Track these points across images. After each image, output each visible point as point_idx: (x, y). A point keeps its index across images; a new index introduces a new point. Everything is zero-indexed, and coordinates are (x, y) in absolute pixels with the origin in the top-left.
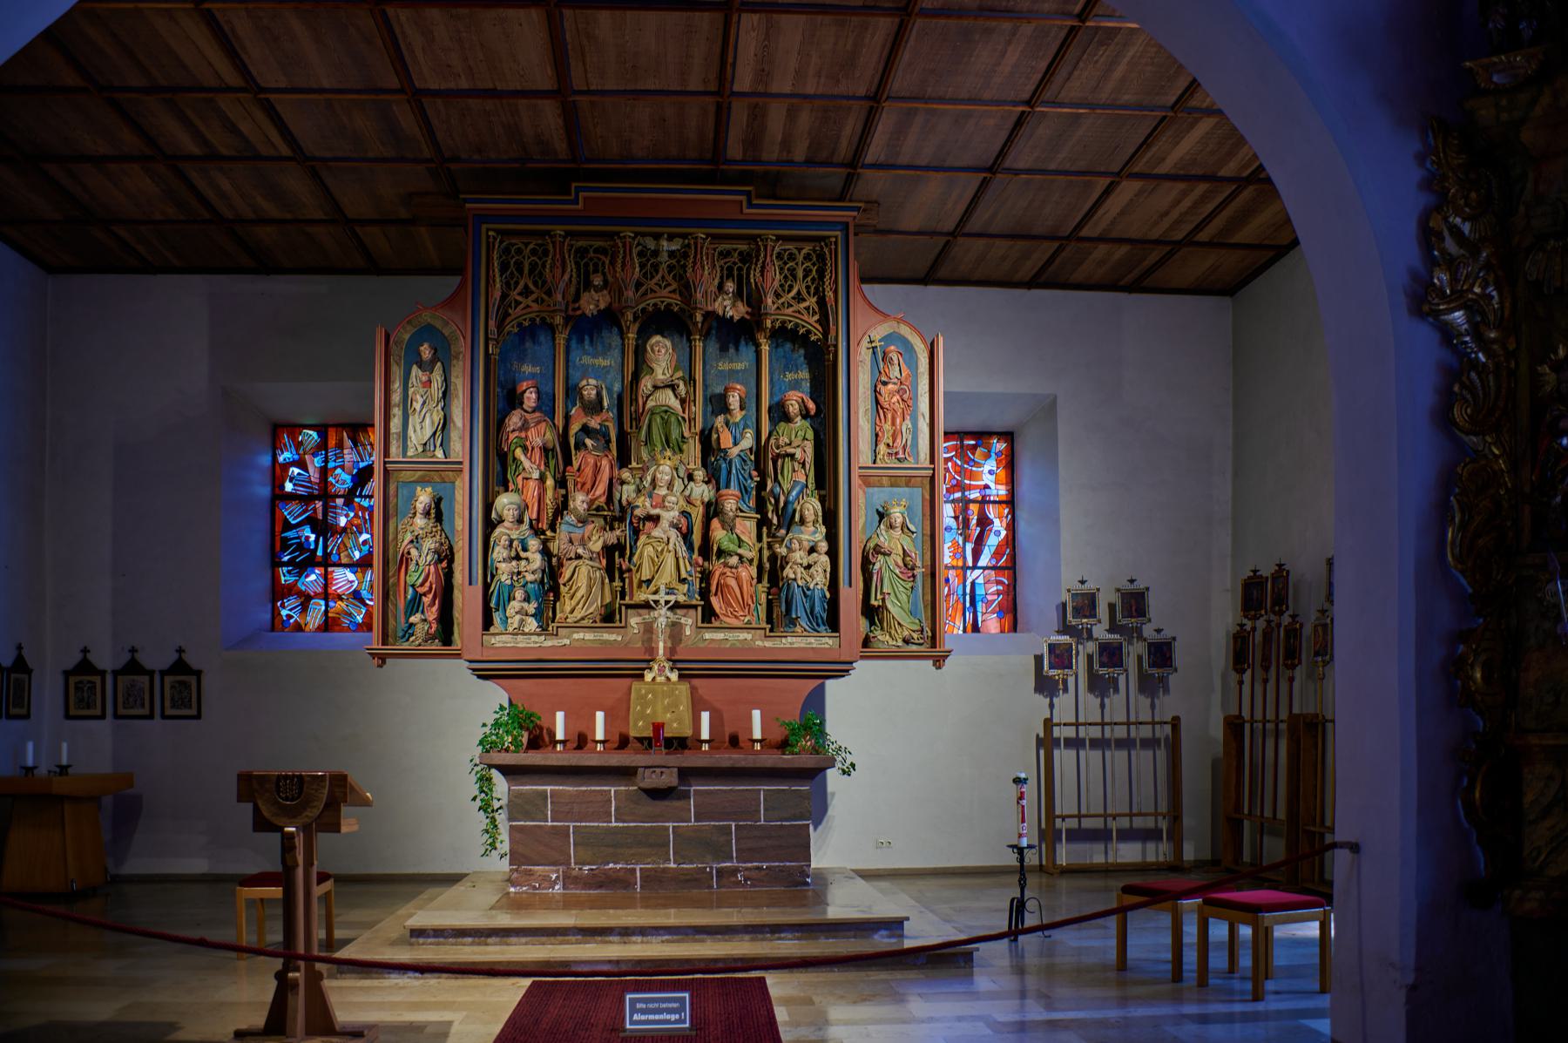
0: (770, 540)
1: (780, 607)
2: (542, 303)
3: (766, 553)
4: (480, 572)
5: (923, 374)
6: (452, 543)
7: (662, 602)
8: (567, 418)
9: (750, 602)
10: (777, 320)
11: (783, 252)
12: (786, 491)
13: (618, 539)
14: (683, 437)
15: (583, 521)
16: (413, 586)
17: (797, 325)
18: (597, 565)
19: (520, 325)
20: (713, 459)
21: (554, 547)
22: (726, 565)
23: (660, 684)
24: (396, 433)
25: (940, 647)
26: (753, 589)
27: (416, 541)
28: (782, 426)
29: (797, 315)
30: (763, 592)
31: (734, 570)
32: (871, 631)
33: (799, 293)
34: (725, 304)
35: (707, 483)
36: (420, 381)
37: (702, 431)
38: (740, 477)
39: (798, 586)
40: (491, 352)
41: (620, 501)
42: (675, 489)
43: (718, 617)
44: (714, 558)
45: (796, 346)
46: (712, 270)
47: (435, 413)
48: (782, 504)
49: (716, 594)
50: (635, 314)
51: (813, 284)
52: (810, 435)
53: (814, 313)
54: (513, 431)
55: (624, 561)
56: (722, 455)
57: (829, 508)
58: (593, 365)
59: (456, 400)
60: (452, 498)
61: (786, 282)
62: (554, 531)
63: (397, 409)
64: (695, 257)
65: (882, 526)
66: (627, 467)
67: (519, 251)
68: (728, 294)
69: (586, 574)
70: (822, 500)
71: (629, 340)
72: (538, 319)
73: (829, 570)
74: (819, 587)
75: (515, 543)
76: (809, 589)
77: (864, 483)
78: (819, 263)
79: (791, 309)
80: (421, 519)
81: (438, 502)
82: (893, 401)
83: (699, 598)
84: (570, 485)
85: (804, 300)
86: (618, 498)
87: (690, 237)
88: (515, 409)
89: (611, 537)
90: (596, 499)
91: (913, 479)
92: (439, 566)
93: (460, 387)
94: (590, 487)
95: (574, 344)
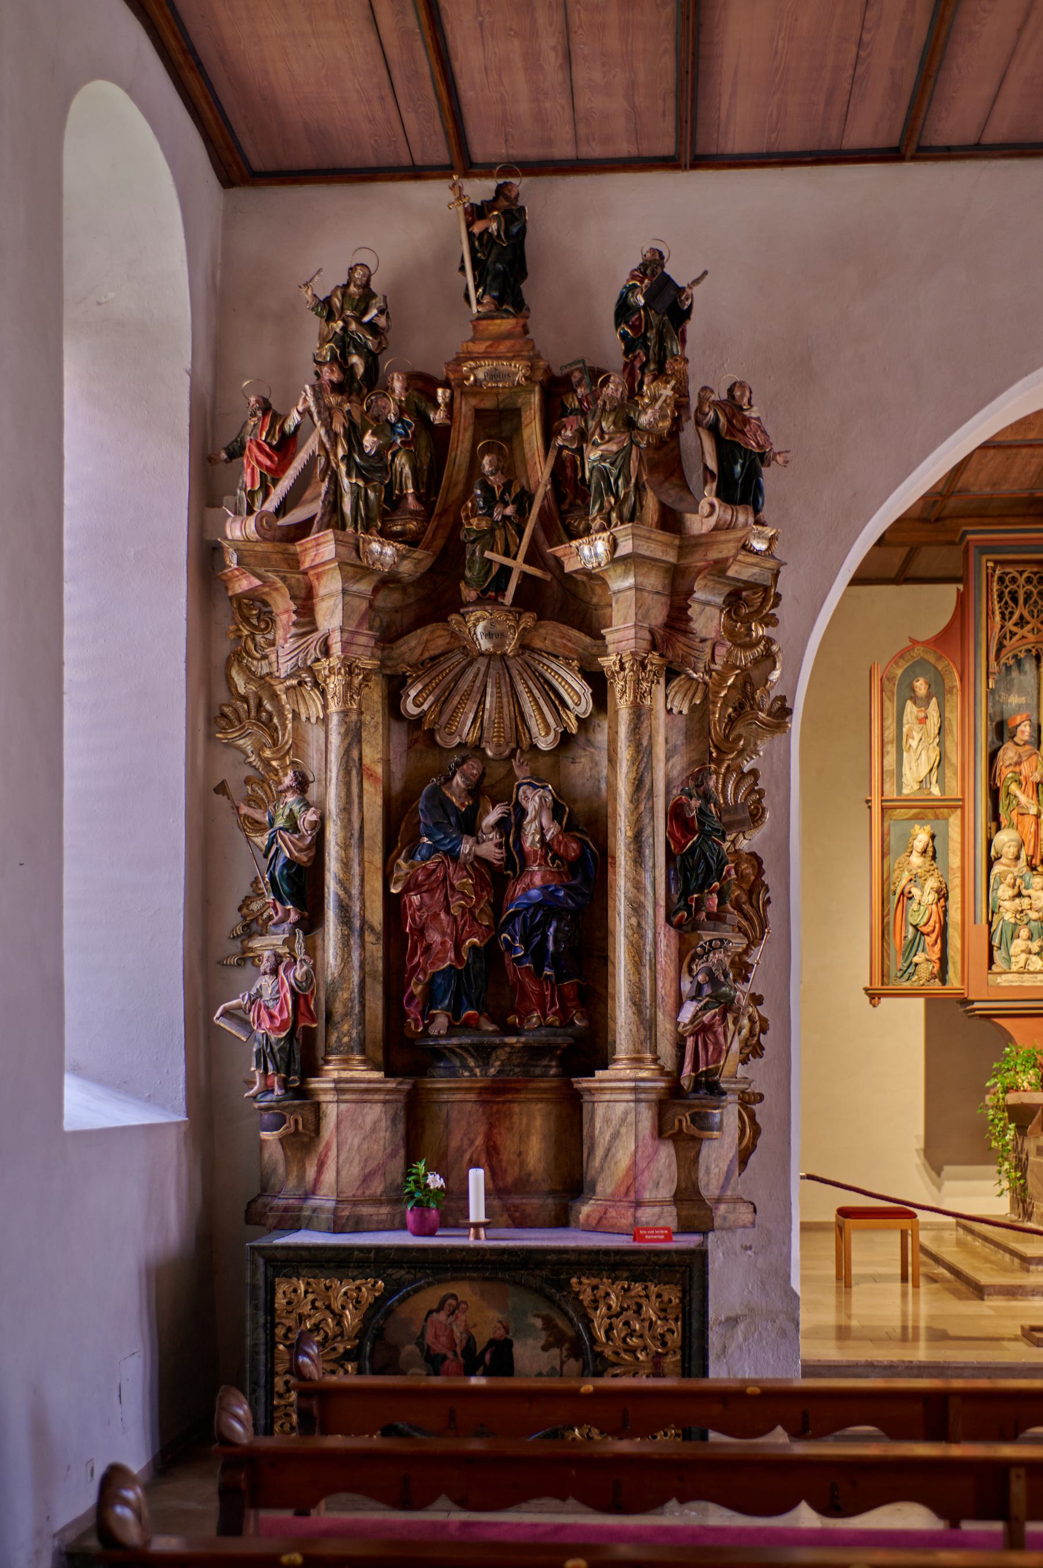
60: (946, 837)
67: (1014, 580)
93: (954, 723)
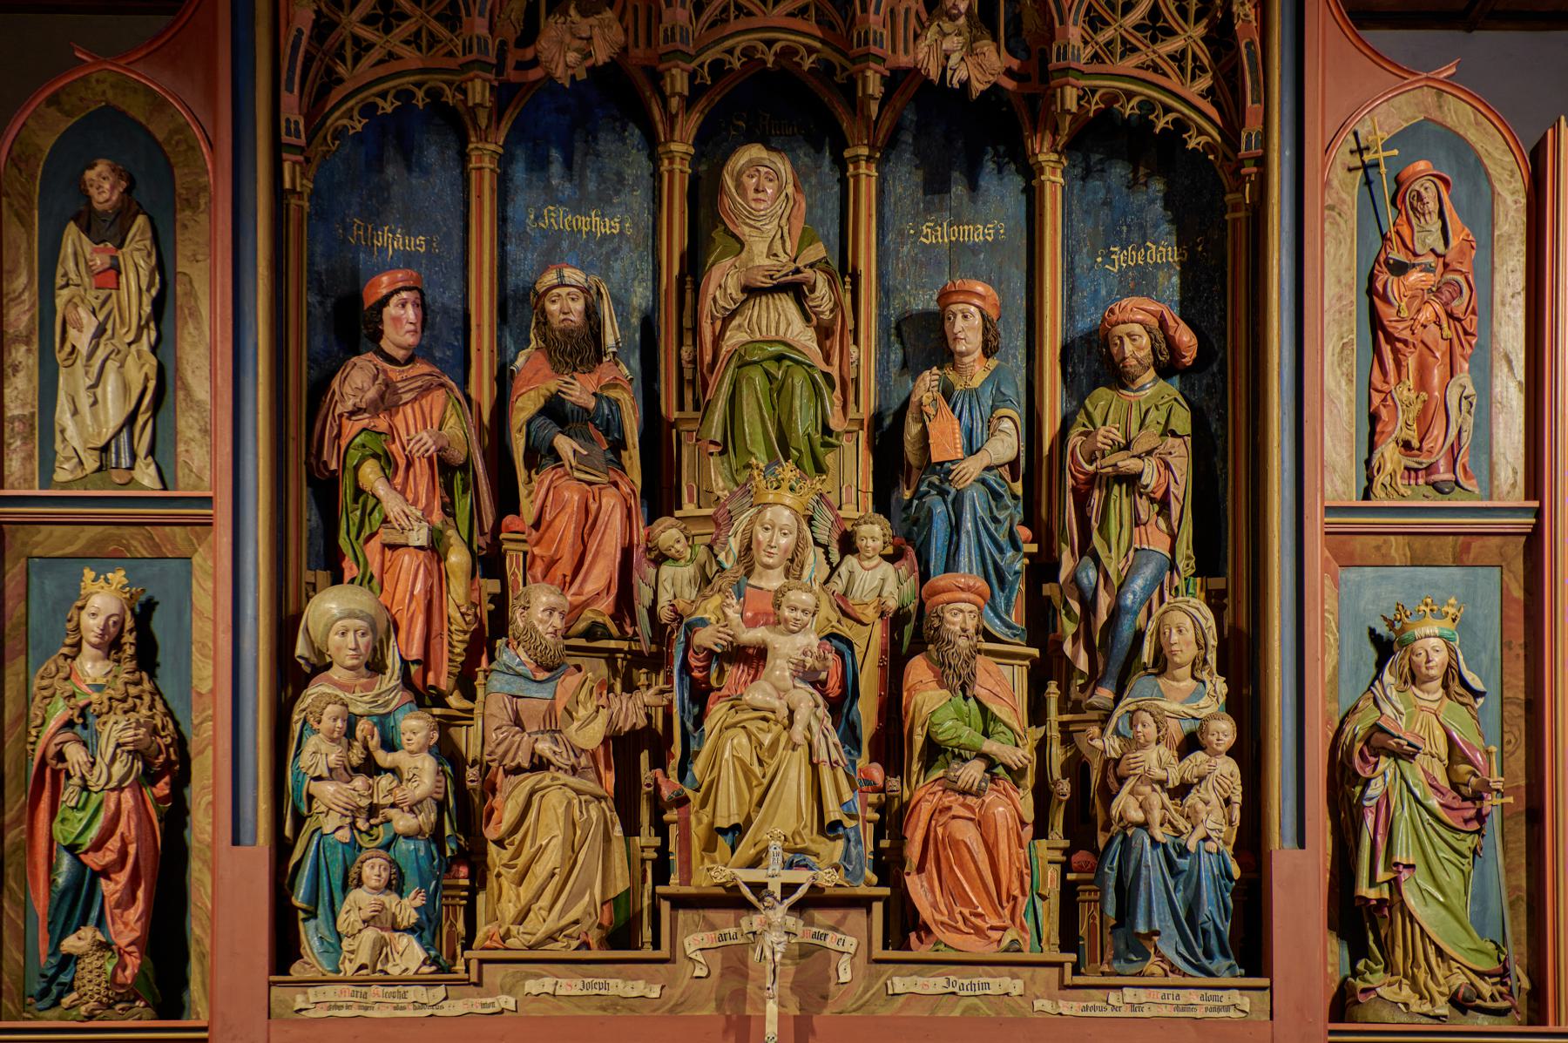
0: (1066, 717)
2: (430, 47)
3: (1057, 755)
4: (264, 806)
5: (1510, 238)
6: (182, 728)
8: (504, 379)
9: (1017, 892)
10: (1094, 91)
12: (1113, 577)
13: (649, 716)
14: (827, 430)
15: (552, 667)
16: (72, 849)
17: (1148, 105)
18: (590, 785)
19: (368, 110)
20: (907, 495)
21: (468, 740)
22: (950, 786)
24: (21, 418)
25: (1557, 1022)
26: (1024, 853)
27: (81, 722)
28: (1103, 395)
29: (1150, 75)
30: (1050, 862)
31: (970, 800)
32: (1355, 973)
33: (1155, 12)
34: (947, 45)
35: (891, 559)
36: (88, 267)
37: (877, 418)
38: (986, 540)
39: (1153, 840)
40: (287, 185)
41: (652, 611)
42: (806, 573)
43: (929, 931)
44: (915, 767)
45: (1142, 171)
47: (131, 362)
48: (1103, 616)
49: (921, 869)
50: (693, 76)
52: (1182, 420)
53: (1199, 69)
54: (352, 413)
55: (666, 775)
56: (935, 479)
57: (1235, 629)
58: (575, 233)
59: (191, 327)
62: (470, 695)
63: (23, 348)
65: (1387, 677)
66: (672, 515)
68: (953, 18)
69: (561, 811)
70: (1215, 601)
71: (671, 161)
72: (420, 94)
73: (1237, 798)
74: (1212, 847)
75: (362, 727)
76: (1183, 852)
77: (1336, 557)
80: (95, 660)
81: (144, 612)
82: (1422, 317)
83: (875, 879)
84: (513, 567)
85: (1170, 33)
86: (647, 602)
88: (358, 353)
89: (631, 711)
90: (585, 604)
91: (1477, 544)
92: (147, 792)
93: (202, 288)
94: (569, 573)
95: (519, 172)
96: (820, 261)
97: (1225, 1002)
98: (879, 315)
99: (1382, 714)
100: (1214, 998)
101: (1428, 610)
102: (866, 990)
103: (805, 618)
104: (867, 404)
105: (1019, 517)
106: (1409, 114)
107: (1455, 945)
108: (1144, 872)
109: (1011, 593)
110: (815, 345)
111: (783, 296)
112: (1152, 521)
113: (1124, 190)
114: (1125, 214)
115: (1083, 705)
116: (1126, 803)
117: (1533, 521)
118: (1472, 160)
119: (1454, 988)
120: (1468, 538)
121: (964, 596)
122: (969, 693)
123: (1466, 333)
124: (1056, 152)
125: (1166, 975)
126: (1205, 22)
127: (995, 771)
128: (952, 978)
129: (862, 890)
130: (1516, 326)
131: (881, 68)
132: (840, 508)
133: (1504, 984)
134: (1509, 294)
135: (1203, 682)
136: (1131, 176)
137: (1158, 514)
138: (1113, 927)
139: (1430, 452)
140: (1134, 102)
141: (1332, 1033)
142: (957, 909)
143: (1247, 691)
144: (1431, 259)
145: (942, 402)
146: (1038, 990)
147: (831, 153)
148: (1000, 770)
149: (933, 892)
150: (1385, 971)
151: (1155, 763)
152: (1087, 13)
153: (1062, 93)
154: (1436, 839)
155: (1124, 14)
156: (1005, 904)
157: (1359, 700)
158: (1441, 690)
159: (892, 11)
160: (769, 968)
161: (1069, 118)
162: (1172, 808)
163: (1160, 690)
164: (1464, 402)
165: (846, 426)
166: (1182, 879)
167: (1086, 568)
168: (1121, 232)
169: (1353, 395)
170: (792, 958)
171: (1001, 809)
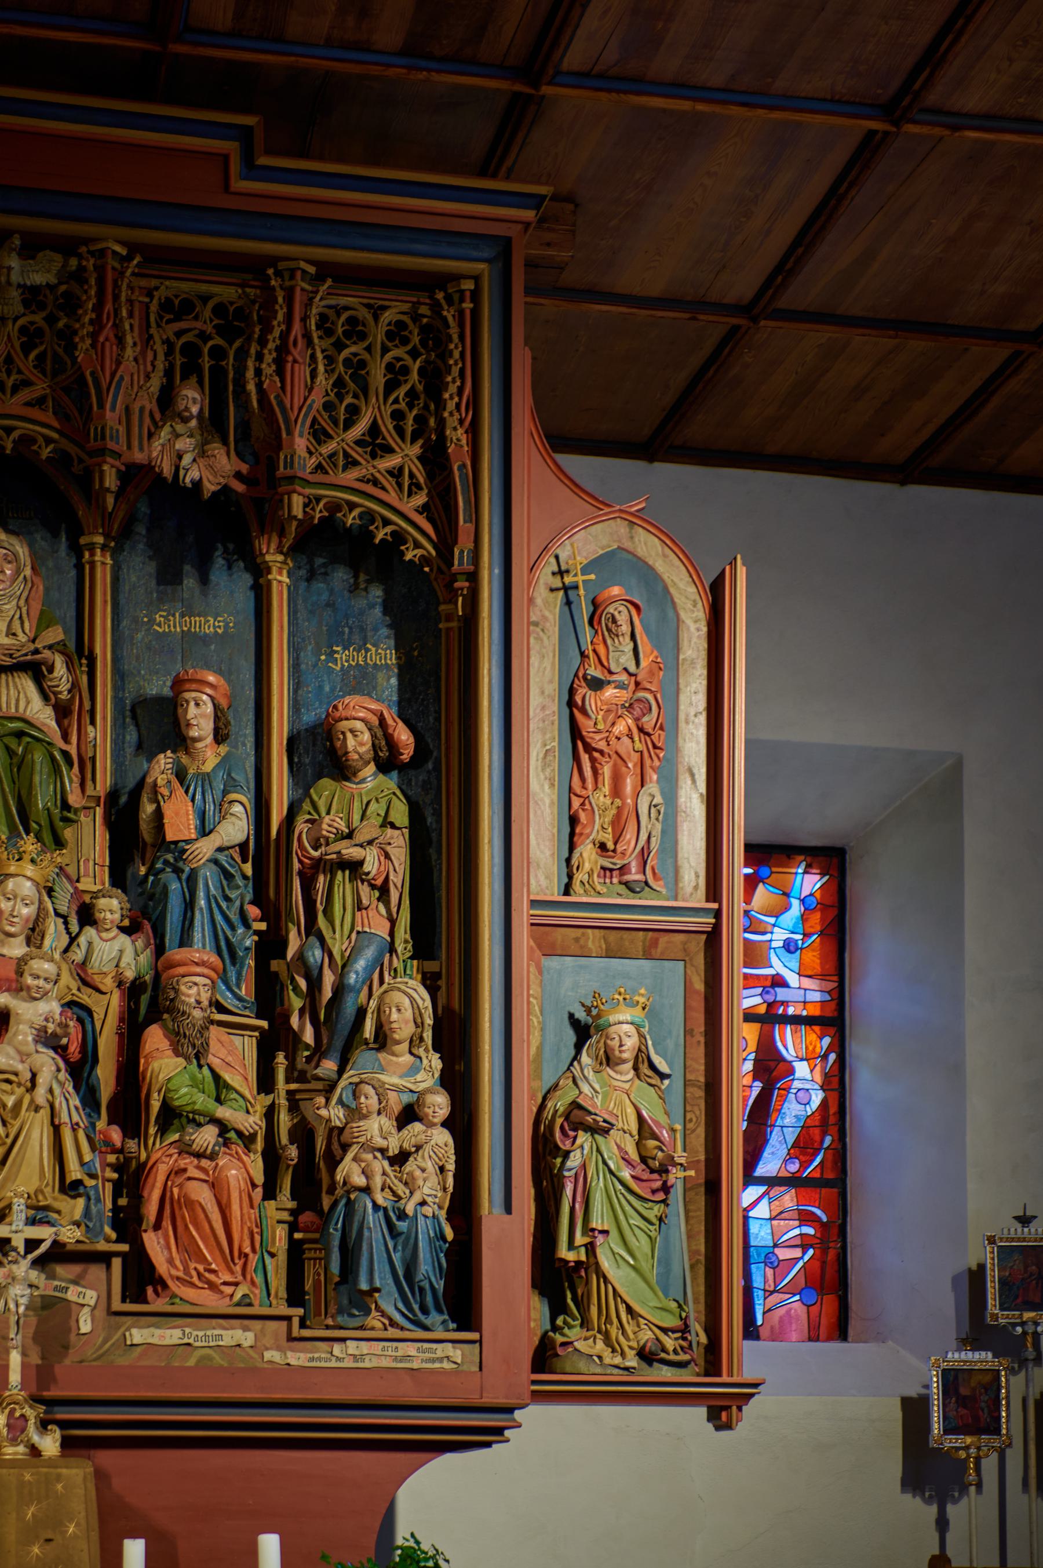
0: (293, 1086)
1: (327, 1259)
3: (284, 1121)
5: (693, 662)
7: (18, 1242)
9: (248, 1250)
10: (318, 499)
11: (331, 313)
14: (66, 806)
17: (369, 516)
20: (143, 870)
22: (185, 1149)
23: (13, 1464)
25: (730, 1374)
26: (254, 1213)
28: (326, 789)
29: (369, 489)
30: (279, 1222)
31: (205, 1163)
33: (374, 429)
34: (179, 445)
37: (113, 796)
38: (219, 918)
39: (376, 1207)
42: (47, 942)
43: (165, 1286)
44: (152, 1130)
45: (362, 577)
46: (143, 353)
48: (327, 993)
49: (157, 1226)
51: (411, 406)
52: (400, 813)
53: (415, 487)
56: (170, 857)
57: (448, 1009)
61: (340, 397)
64: (98, 308)
65: (585, 1058)
68: (185, 420)
70: (430, 982)
73: (451, 1166)
74: (428, 1211)
76: (402, 1215)
78: (428, 352)
79: (354, 474)
85: (389, 450)
87: (83, 249)
91: (664, 939)
96: (58, 643)
97: (439, 1354)
98: (115, 697)
99: (581, 1093)
100: (429, 1350)
101: (621, 998)
102: (105, 1341)
103: (48, 986)
104: (103, 782)
105: (249, 897)
106: (604, 542)
107: (644, 1303)
108: (366, 1233)
109: (242, 967)
110: (54, 724)
111: (23, 675)
112: (373, 906)
113: (346, 594)
114: (347, 617)
115: (309, 1075)
116: (350, 1169)
117: (713, 921)
118: (660, 588)
119: (642, 1343)
120: (656, 934)
121: (198, 970)
122: (202, 1062)
123: (655, 747)
124: (281, 553)
125: (386, 1329)
126: (420, 442)
127: (228, 1135)
128: (187, 1330)
129: (102, 1246)
130: (698, 743)
131: (117, 463)
132: (78, 881)
133: (684, 1339)
134: (693, 713)
135: (420, 1058)
136: (352, 581)
137: (379, 899)
138: (337, 1284)
139: (623, 853)
140: (356, 512)
141: (534, 1382)
142: (192, 1265)
143: (460, 1067)
144: (624, 677)
145: (176, 784)
146: (268, 1341)
147: (67, 539)
148: (232, 1135)
149: (169, 1248)
150: (582, 1326)
151: (376, 1132)
152: (312, 426)
153: (289, 499)
154: (628, 1208)
155: (346, 428)
156: (237, 1261)
157: (560, 1079)
158: (632, 1073)
159: (127, 409)
160: (13, 1319)
161: (295, 523)
162: (391, 1174)
163: (380, 1064)
164: (653, 810)
165: (84, 803)
166: (401, 1240)
167: (312, 948)
168: (343, 633)
169: (555, 797)
170: (34, 1310)
171: (234, 1172)
